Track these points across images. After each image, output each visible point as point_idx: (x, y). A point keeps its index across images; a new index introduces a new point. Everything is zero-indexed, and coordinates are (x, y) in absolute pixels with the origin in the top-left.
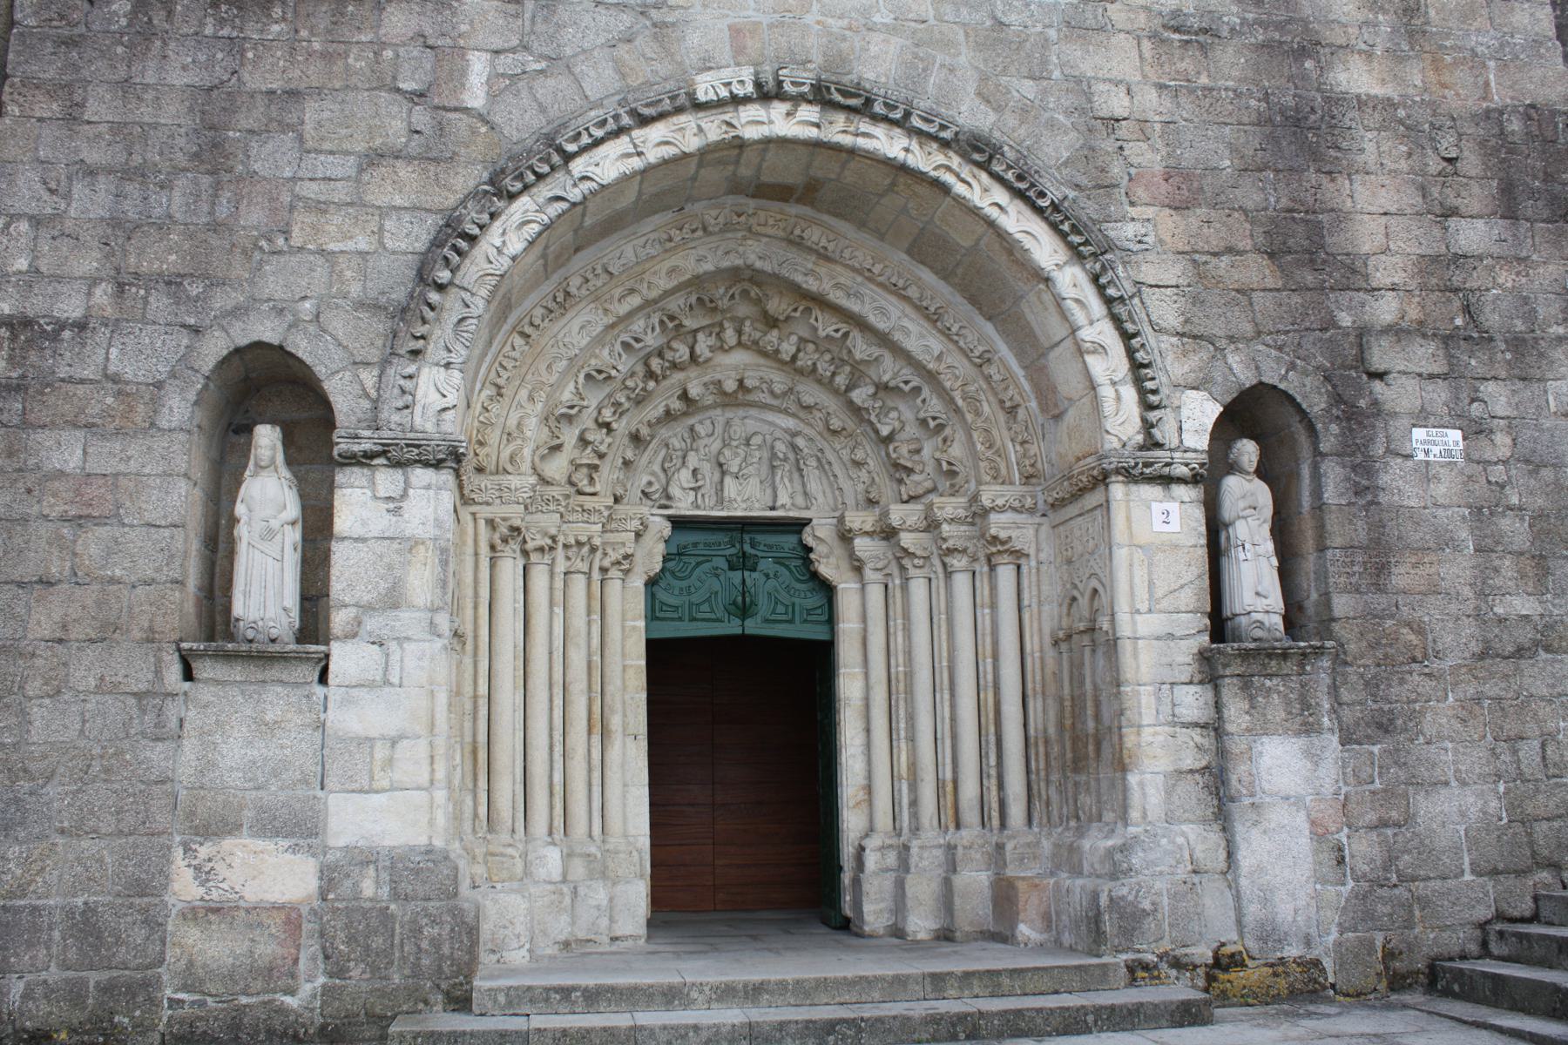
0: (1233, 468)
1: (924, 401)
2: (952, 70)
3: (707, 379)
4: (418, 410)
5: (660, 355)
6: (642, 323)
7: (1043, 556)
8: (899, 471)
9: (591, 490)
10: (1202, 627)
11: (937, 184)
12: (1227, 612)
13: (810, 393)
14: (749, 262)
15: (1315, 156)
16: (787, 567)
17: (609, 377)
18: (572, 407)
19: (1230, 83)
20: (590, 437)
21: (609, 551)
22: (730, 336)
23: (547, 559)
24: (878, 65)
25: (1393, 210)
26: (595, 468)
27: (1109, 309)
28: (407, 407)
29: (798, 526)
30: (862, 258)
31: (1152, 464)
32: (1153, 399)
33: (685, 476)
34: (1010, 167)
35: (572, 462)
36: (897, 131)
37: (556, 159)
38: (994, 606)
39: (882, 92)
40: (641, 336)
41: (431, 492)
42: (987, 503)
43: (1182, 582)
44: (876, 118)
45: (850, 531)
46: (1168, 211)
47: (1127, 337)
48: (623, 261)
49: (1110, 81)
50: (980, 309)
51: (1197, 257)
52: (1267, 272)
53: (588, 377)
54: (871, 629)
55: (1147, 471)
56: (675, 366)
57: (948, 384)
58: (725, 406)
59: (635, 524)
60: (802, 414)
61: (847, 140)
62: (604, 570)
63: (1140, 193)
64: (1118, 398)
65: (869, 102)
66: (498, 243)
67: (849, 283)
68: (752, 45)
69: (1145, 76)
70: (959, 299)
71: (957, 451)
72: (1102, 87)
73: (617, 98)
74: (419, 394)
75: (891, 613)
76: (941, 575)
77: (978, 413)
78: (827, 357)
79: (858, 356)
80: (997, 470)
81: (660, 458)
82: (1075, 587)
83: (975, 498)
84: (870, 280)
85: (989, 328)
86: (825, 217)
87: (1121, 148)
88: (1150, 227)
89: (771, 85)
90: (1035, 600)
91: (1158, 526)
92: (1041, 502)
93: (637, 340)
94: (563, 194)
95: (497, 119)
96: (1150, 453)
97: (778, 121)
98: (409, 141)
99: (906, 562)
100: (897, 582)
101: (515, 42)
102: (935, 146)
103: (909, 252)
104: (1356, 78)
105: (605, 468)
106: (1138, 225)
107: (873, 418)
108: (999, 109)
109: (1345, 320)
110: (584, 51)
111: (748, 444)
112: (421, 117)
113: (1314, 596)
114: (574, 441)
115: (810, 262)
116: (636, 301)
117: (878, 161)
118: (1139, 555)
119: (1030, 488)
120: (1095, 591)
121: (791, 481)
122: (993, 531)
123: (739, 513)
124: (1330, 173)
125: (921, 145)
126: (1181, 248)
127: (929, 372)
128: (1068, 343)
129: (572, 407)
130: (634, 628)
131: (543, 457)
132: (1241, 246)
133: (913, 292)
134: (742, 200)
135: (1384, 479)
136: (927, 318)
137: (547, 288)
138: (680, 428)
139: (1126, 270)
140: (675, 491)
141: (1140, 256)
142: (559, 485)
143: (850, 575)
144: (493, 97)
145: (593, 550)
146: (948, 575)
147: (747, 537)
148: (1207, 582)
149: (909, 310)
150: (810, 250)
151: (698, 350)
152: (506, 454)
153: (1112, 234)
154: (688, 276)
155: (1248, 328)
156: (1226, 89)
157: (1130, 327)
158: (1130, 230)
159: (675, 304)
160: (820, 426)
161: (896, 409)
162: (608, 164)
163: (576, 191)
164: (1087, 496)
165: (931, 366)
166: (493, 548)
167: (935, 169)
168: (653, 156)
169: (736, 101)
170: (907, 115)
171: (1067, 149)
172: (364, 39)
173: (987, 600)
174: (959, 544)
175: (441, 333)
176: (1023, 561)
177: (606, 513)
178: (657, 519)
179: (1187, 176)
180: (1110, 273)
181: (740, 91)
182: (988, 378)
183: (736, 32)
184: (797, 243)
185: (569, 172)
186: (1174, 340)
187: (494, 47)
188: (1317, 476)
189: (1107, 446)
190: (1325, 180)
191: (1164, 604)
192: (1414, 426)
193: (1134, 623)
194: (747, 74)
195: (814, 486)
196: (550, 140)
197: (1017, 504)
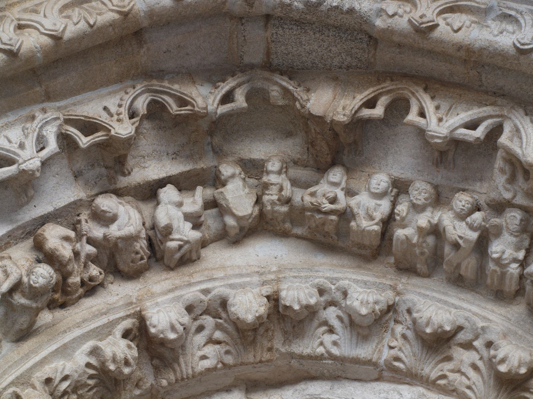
3: (192, 294)
5: (75, 226)
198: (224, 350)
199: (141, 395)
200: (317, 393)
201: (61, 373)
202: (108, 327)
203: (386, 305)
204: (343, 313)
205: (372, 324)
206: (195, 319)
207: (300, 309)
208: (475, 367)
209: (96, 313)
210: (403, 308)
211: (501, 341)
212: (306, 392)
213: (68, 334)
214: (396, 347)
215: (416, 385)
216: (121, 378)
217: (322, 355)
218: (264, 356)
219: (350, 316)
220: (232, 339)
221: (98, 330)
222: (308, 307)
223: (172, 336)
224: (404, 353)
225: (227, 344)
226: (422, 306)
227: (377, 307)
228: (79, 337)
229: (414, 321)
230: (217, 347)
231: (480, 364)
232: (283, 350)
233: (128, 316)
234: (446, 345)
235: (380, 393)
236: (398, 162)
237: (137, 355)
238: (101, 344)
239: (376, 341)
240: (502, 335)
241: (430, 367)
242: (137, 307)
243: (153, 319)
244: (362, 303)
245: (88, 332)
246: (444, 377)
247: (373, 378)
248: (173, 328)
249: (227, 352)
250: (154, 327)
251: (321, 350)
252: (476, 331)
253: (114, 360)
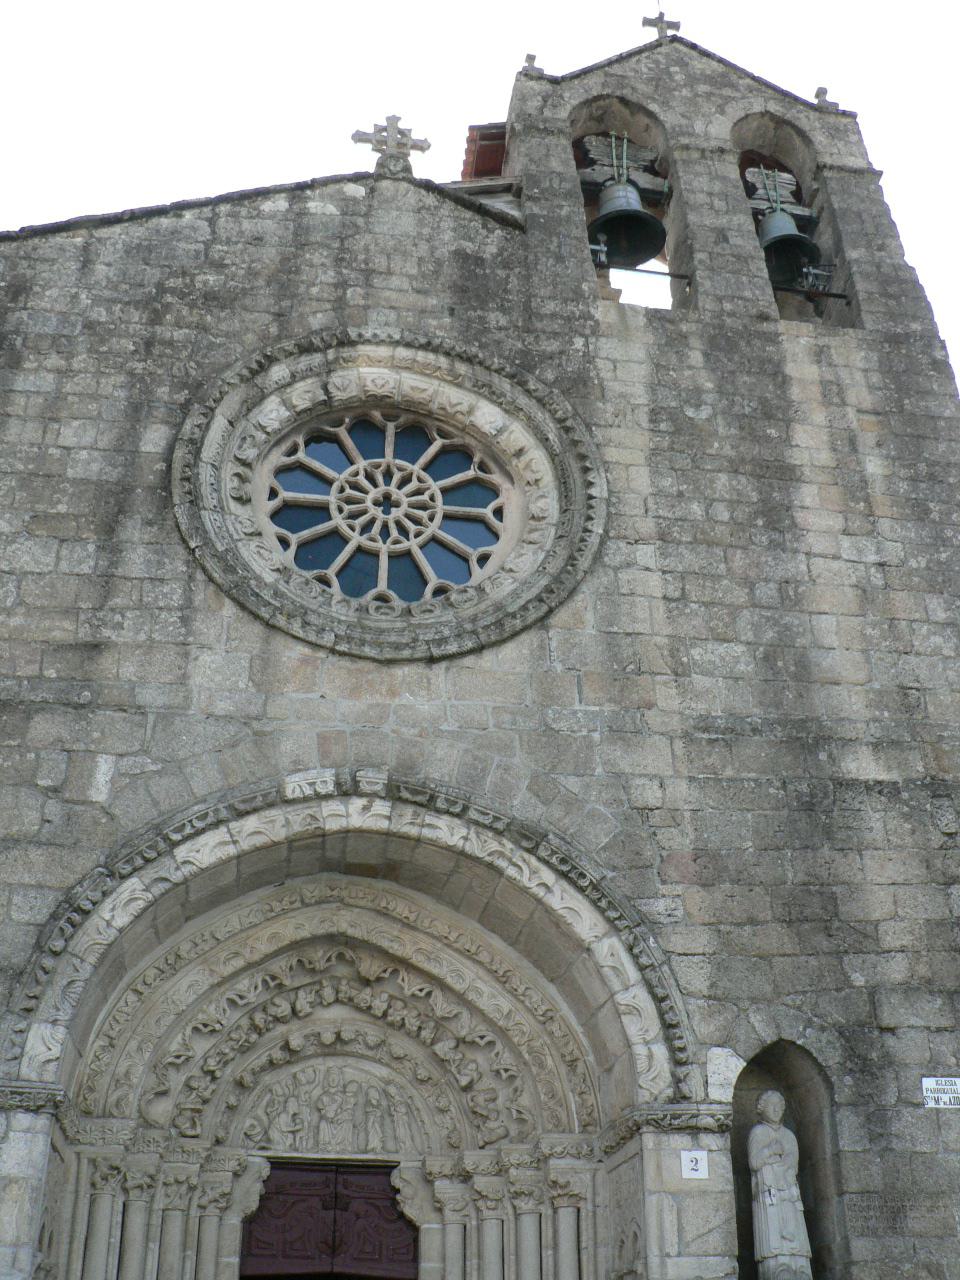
0: (762, 1118)
1: (497, 1054)
2: (507, 770)
3: (307, 1031)
4: (25, 1060)
5: (264, 1010)
6: (246, 982)
7: (599, 1200)
8: (477, 1117)
9: (193, 1133)
10: (730, 1271)
11: (490, 866)
12: (758, 1257)
13: (400, 1044)
14: (341, 931)
15: (828, 834)
16: (377, 1207)
17: (213, 1031)
18: (178, 1057)
19: (753, 775)
20: (194, 1084)
21: (208, 1191)
22: (328, 994)
23: (145, 1196)
24: (442, 765)
25: (900, 880)
26: (199, 1111)
27: (643, 975)
28: (16, 1058)
29: (387, 1169)
30: (441, 928)
31: (680, 1116)
32: (682, 1056)
33: (284, 1121)
34: (554, 853)
35: (177, 1106)
36: (457, 821)
37: (162, 845)
38: (556, 1247)
39: (444, 790)
40: (245, 994)
41: (29, 1135)
42: (547, 1151)
43: (711, 1226)
44: (438, 811)
45: (430, 1174)
46: (696, 888)
47: (659, 1000)
48: (227, 929)
49: (645, 776)
50: (543, 972)
51: (722, 927)
52: (786, 939)
53: (196, 1029)
54: (448, 1269)
55: (676, 1122)
56: (277, 1020)
57: (516, 1040)
58: (326, 1055)
59: (233, 1165)
60: (394, 1064)
61: (413, 831)
62: (202, 1207)
63: (672, 873)
64: (650, 1056)
65: (433, 798)
66: (107, 916)
67: (429, 948)
68: (336, 751)
69: (676, 771)
70: (525, 963)
71: (525, 1100)
72: (639, 781)
73: (219, 794)
74: (27, 1049)
75: (468, 1254)
76: (512, 1218)
77: (542, 1066)
78: (415, 1013)
79: (439, 1013)
80: (559, 1120)
81: (264, 1102)
82: (623, 1232)
83: (537, 1146)
84: (449, 946)
85: (552, 990)
86: (409, 892)
87: (655, 834)
88: (679, 902)
89: (347, 787)
90: (591, 1243)
91: (687, 1174)
92: (597, 1151)
93: (241, 997)
94: (168, 876)
95: (117, 812)
96: (676, 1106)
97: (353, 815)
98: (42, 826)
99: (480, 1203)
100: (474, 1223)
101: (137, 747)
102: (490, 834)
103: (480, 921)
104: (863, 766)
105: (208, 1110)
106: (669, 901)
107: (453, 1069)
108: (546, 802)
109: (859, 980)
110: (194, 755)
111: (344, 1092)
112: (53, 809)
113: (838, 1239)
114: (180, 1087)
115: (395, 930)
116: (239, 963)
117: (441, 848)
118: (668, 1202)
119: (587, 1136)
120: (635, 1234)
121: (382, 1125)
122: (552, 1177)
124: (842, 850)
125: (477, 834)
126: (707, 920)
127: (500, 1028)
128: (609, 1005)
129: (178, 1057)
130: (228, 1265)
131: (149, 1102)
132: (761, 917)
133: (484, 957)
134: (336, 876)
135: (896, 1127)
136: (497, 979)
137: (160, 951)
138: (284, 1075)
139: (657, 942)
140: (274, 1135)
141: (670, 928)
142: (162, 1128)
143: (433, 1216)
144: (116, 793)
145: (192, 1188)
146: (517, 1216)
147: (341, 1178)
148: (734, 1226)
149: (482, 973)
150: (395, 919)
151: (298, 1007)
152: (113, 1098)
153: (644, 909)
154: (286, 942)
155: (768, 989)
156: (749, 780)
157: (660, 992)
158: (660, 906)
159: (279, 966)
161: (474, 1061)
162: (206, 851)
163: (179, 873)
164: (628, 1144)
165: (501, 1023)
166: (93, 1185)
167: (489, 855)
168: (245, 845)
169: (320, 797)
170: (465, 809)
171: (606, 835)
172: (13, 743)
173: (551, 1242)
174: (525, 1189)
175: (52, 996)
176: (581, 1204)
177: (204, 1154)
178: (257, 1160)
179: (715, 856)
180: (642, 944)
181: (322, 790)
182: (551, 1034)
183: (323, 739)
184: (384, 914)
185: (174, 857)
186: (701, 1002)
187: (119, 751)
188: (834, 1126)
189: (641, 1100)
190: (838, 856)
191: (693, 1248)
192: (924, 1076)
193: (663, 1264)
194: (329, 775)
195: (402, 1132)
196: (157, 829)
197: (574, 1151)
236: (389, 989)
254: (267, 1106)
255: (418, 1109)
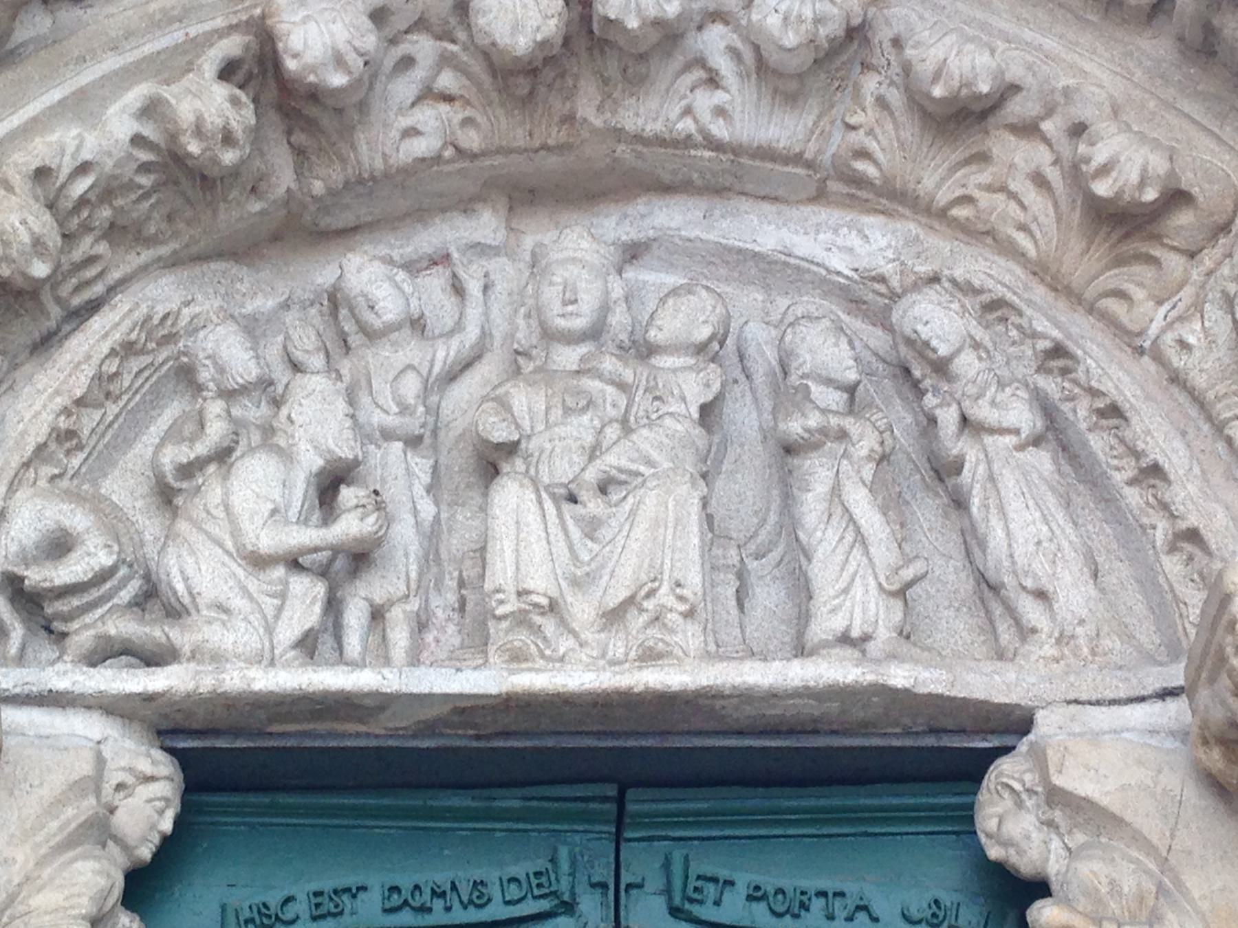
33: (260, 497)
60: (935, 177)
123: (578, 677)
160: (1041, 221)
198: (460, 116)
199: (262, 213)
200: (673, 225)
201: (73, 156)
202: (185, 52)
203: (844, 26)
204: (742, 41)
205: (810, 68)
206: (393, 41)
207: (640, 28)
208: (1039, 180)
209: (158, 17)
210: (883, 35)
211: (1105, 125)
212: (648, 222)
213: (89, 64)
214: (861, 126)
215: (902, 216)
216: (214, 172)
217: (689, 137)
218: (554, 133)
219: (757, 48)
220: (480, 88)
221: (163, 57)
222: (658, 23)
223: (338, 80)
224: (879, 142)
225: (468, 103)
226: (927, 33)
227: (823, 31)
228: (116, 73)
229: (907, 69)
230: (444, 108)
231: (1053, 174)
232: (598, 122)
233: (232, 28)
234: (977, 127)
235: (818, 232)
237: (253, 122)
238: (166, 93)
239: (816, 111)
240: (1108, 110)
241: (937, 177)
242: (255, 6)
243: (292, 37)
244: (785, 19)
245: (138, 64)
246: (967, 200)
247: (804, 195)
248: (339, 61)
249: (467, 122)
250: (295, 56)
251: (686, 126)
252: (1049, 98)
253: (199, 131)
254: (173, 435)
255: (1114, 412)
